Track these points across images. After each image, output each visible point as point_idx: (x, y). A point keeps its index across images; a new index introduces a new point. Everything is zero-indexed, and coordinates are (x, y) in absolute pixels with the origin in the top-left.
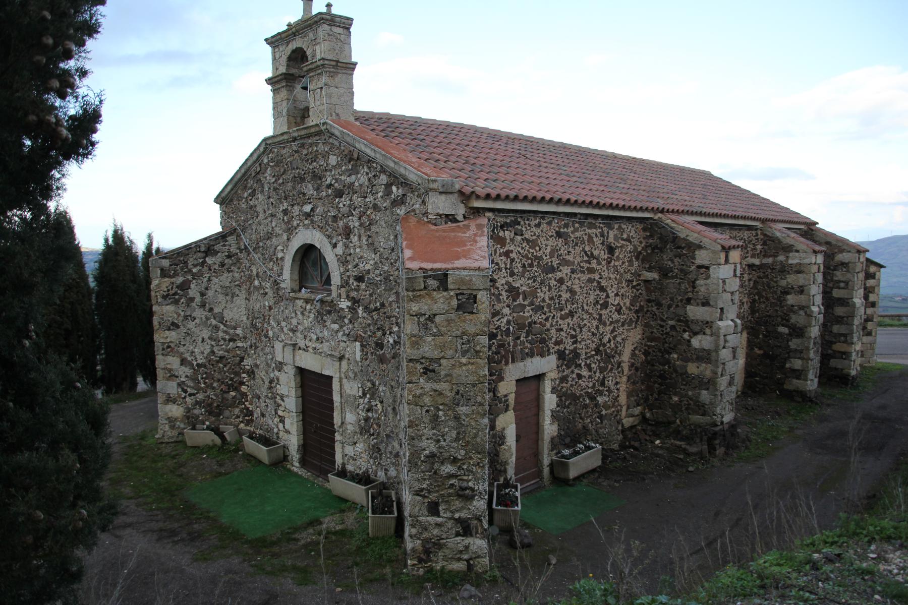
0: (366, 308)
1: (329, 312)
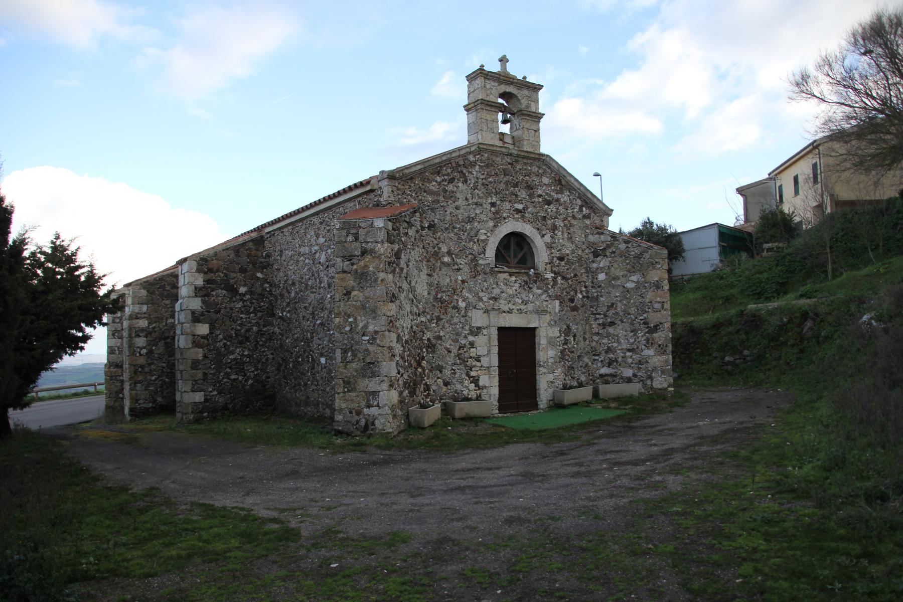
0: (564, 278)
1: (535, 282)
